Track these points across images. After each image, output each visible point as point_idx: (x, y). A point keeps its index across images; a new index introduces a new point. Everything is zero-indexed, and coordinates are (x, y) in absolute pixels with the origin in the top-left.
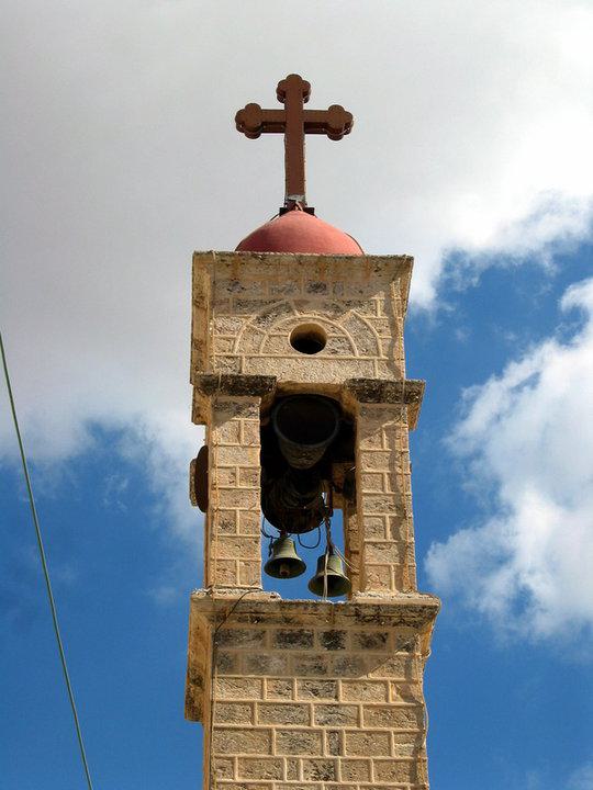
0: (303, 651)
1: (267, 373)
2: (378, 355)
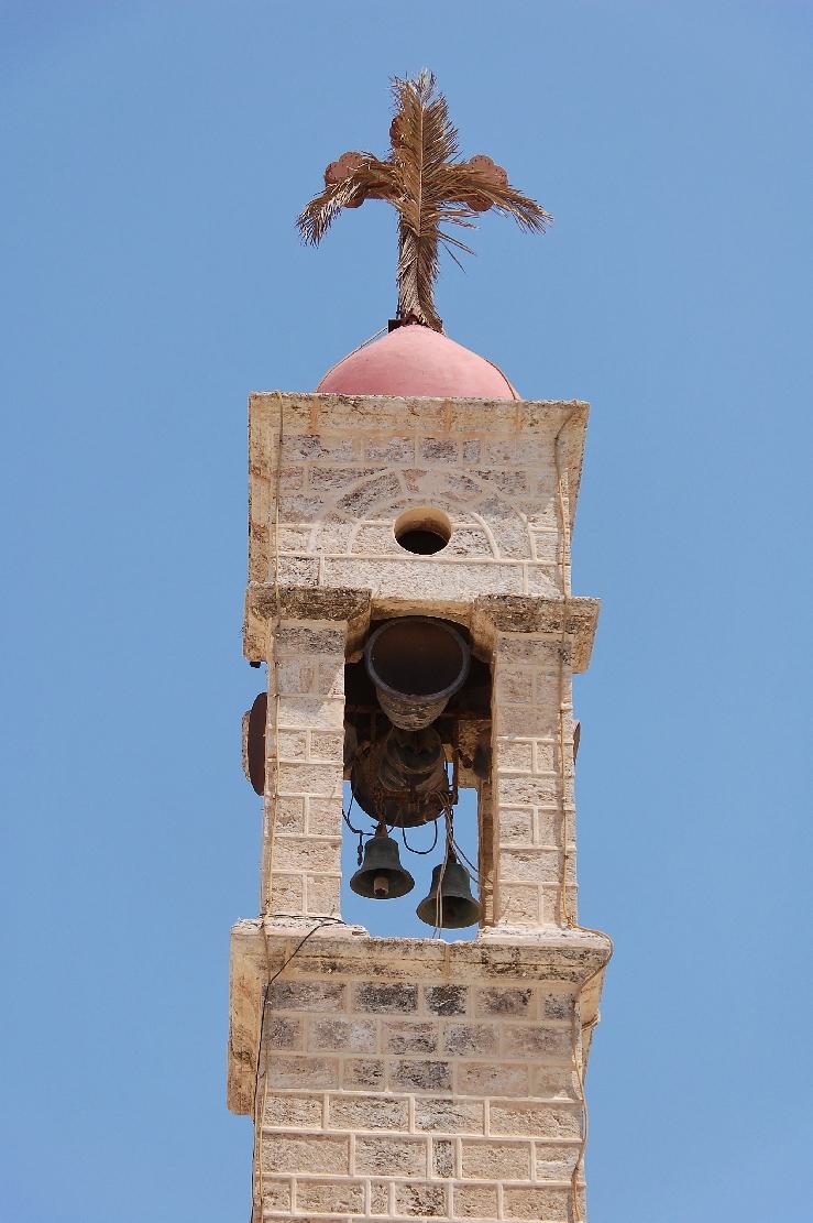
1: (357, 584)
2: (531, 558)
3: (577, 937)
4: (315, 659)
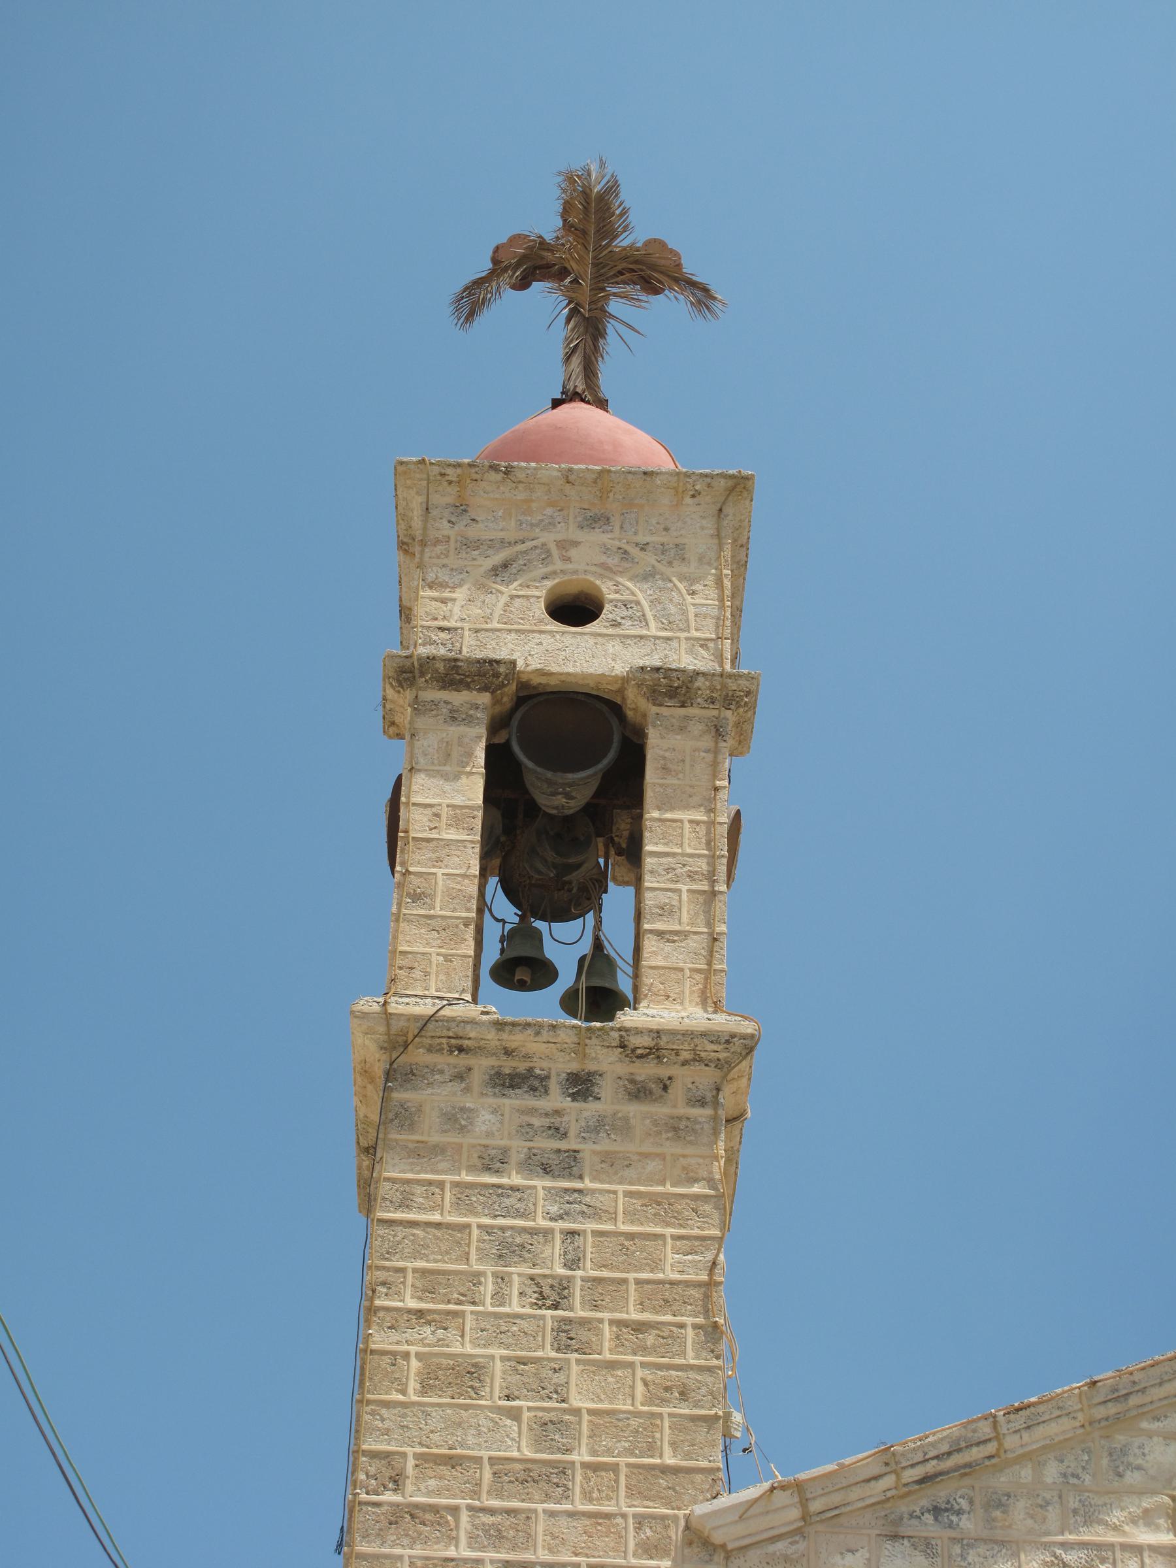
0: (531, 1102)
1: (502, 654)
3: (722, 1022)
4: (455, 730)
